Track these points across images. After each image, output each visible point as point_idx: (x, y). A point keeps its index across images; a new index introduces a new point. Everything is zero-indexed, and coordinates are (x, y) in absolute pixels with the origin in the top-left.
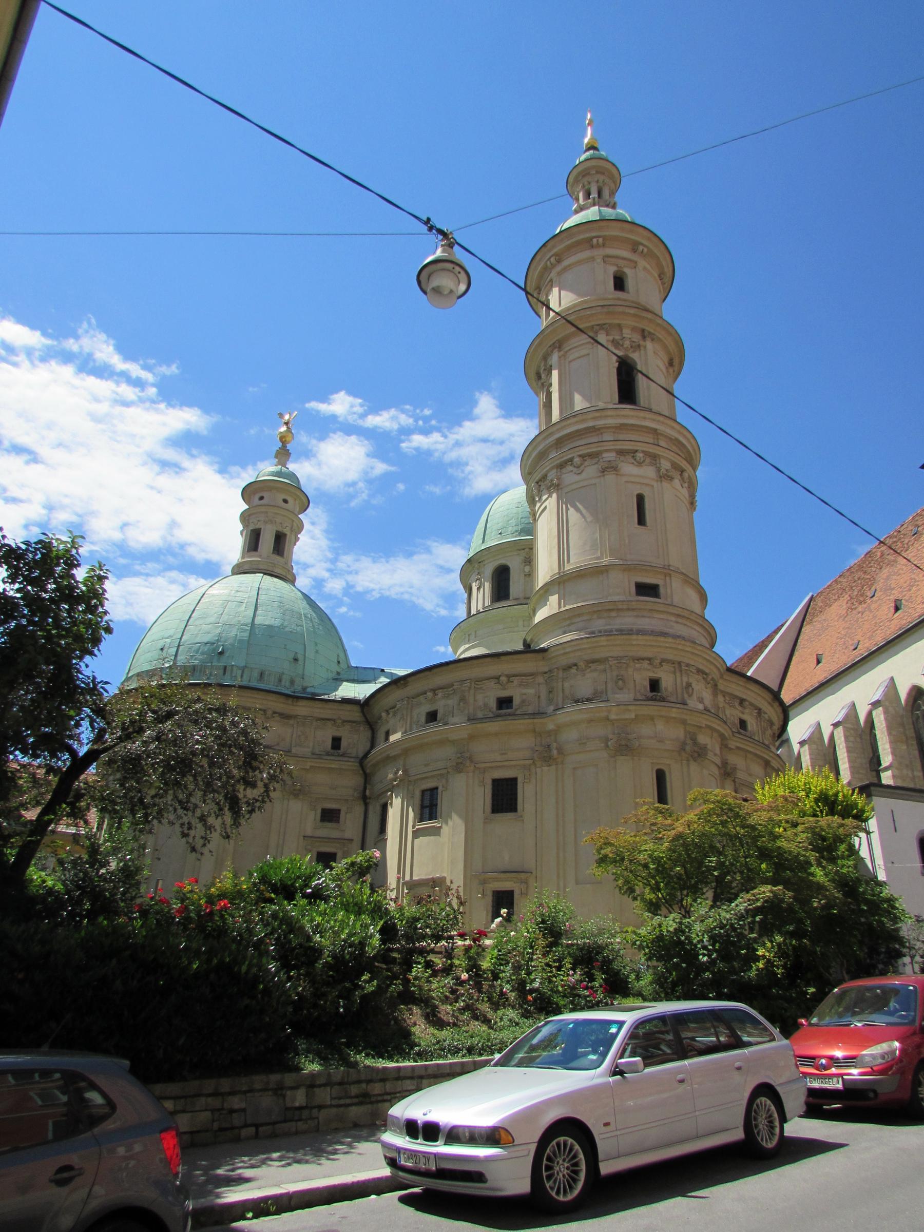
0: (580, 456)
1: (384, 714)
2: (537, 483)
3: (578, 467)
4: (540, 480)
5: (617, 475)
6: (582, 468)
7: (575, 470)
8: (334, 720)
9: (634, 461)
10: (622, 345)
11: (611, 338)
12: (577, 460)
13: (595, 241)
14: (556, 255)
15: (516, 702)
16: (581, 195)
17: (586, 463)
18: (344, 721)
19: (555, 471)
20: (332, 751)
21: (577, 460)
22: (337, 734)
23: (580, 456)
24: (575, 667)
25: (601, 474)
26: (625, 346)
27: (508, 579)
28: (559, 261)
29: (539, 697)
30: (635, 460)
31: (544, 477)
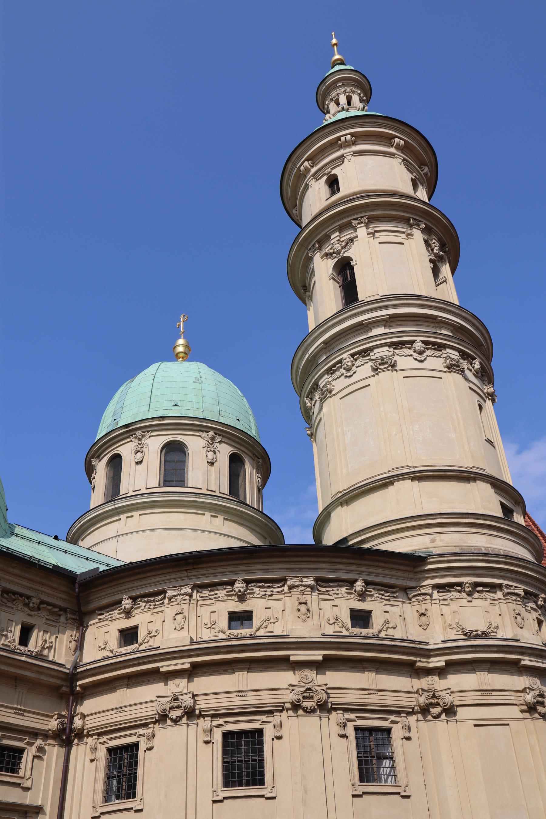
0: (423, 342)
1: (127, 603)
2: (352, 355)
3: (421, 353)
4: (359, 353)
5: (463, 376)
6: (425, 354)
7: (415, 355)
8: (29, 597)
9: (472, 369)
10: (432, 250)
11: (426, 238)
12: (418, 346)
13: (397, 140)
14: (352, 135)
15: (377, 620)
16: (343, 100)
17: (428, 352)
18: (42, 602)
19: (387, 348)
20: (22, 648)
21: (418, 346)
22: (30, 620)
23: (423, 342)
24: (459, 588)
25: (446, 369)
26: (435, 251)
27: (183, 462)
28: (354, 143)
29: (404, 619)
30: (473, 367)
31: (365, 353)
